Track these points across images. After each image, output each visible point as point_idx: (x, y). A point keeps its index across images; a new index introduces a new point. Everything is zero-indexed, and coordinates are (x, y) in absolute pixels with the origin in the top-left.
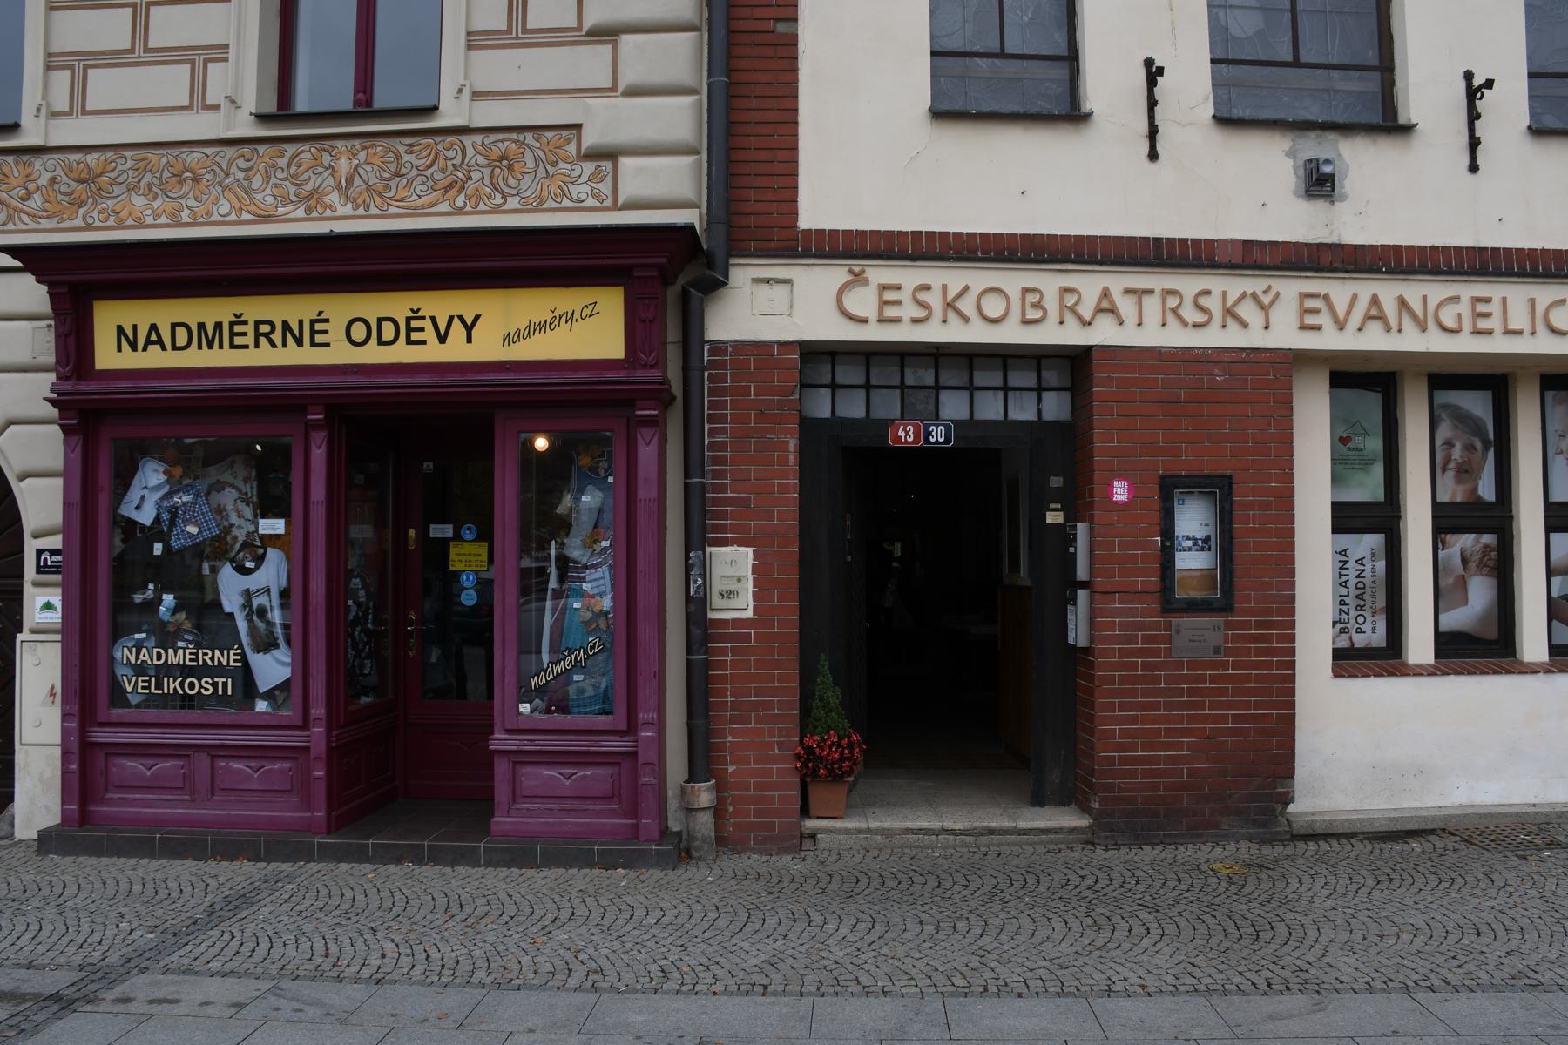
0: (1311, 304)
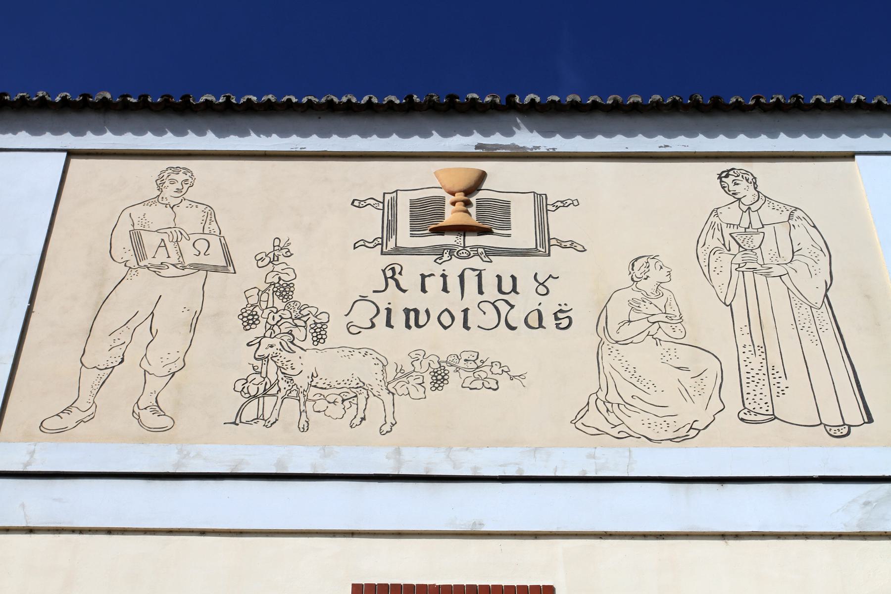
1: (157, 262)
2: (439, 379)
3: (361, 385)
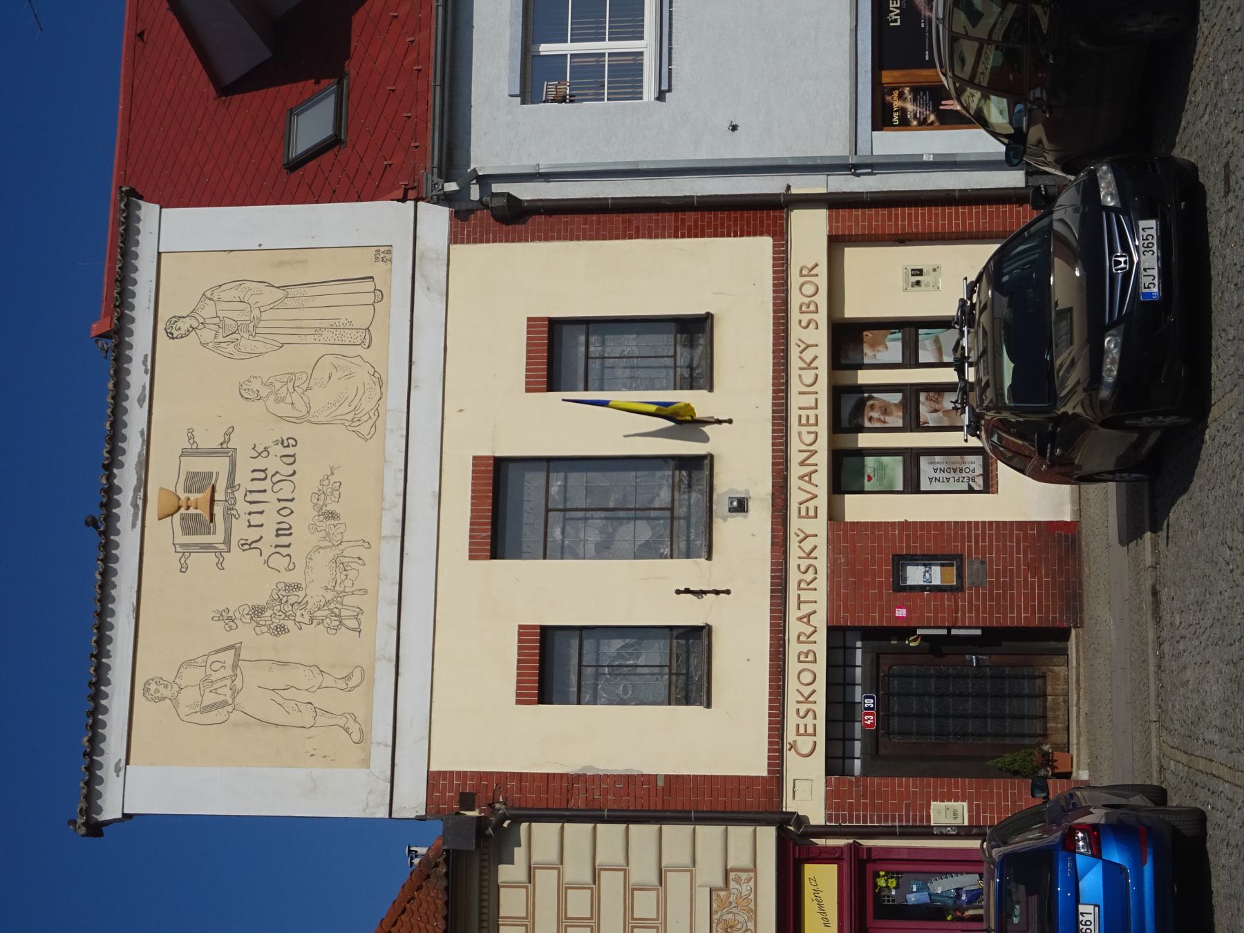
0: (803, 513)
1: (229, 693)
2: (333, 515)
3: (335, 560)
